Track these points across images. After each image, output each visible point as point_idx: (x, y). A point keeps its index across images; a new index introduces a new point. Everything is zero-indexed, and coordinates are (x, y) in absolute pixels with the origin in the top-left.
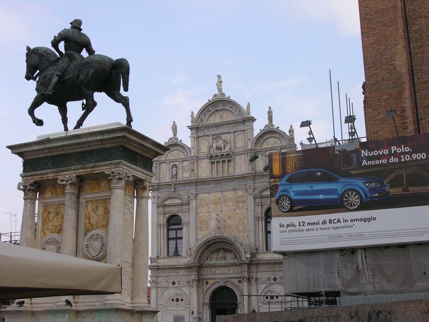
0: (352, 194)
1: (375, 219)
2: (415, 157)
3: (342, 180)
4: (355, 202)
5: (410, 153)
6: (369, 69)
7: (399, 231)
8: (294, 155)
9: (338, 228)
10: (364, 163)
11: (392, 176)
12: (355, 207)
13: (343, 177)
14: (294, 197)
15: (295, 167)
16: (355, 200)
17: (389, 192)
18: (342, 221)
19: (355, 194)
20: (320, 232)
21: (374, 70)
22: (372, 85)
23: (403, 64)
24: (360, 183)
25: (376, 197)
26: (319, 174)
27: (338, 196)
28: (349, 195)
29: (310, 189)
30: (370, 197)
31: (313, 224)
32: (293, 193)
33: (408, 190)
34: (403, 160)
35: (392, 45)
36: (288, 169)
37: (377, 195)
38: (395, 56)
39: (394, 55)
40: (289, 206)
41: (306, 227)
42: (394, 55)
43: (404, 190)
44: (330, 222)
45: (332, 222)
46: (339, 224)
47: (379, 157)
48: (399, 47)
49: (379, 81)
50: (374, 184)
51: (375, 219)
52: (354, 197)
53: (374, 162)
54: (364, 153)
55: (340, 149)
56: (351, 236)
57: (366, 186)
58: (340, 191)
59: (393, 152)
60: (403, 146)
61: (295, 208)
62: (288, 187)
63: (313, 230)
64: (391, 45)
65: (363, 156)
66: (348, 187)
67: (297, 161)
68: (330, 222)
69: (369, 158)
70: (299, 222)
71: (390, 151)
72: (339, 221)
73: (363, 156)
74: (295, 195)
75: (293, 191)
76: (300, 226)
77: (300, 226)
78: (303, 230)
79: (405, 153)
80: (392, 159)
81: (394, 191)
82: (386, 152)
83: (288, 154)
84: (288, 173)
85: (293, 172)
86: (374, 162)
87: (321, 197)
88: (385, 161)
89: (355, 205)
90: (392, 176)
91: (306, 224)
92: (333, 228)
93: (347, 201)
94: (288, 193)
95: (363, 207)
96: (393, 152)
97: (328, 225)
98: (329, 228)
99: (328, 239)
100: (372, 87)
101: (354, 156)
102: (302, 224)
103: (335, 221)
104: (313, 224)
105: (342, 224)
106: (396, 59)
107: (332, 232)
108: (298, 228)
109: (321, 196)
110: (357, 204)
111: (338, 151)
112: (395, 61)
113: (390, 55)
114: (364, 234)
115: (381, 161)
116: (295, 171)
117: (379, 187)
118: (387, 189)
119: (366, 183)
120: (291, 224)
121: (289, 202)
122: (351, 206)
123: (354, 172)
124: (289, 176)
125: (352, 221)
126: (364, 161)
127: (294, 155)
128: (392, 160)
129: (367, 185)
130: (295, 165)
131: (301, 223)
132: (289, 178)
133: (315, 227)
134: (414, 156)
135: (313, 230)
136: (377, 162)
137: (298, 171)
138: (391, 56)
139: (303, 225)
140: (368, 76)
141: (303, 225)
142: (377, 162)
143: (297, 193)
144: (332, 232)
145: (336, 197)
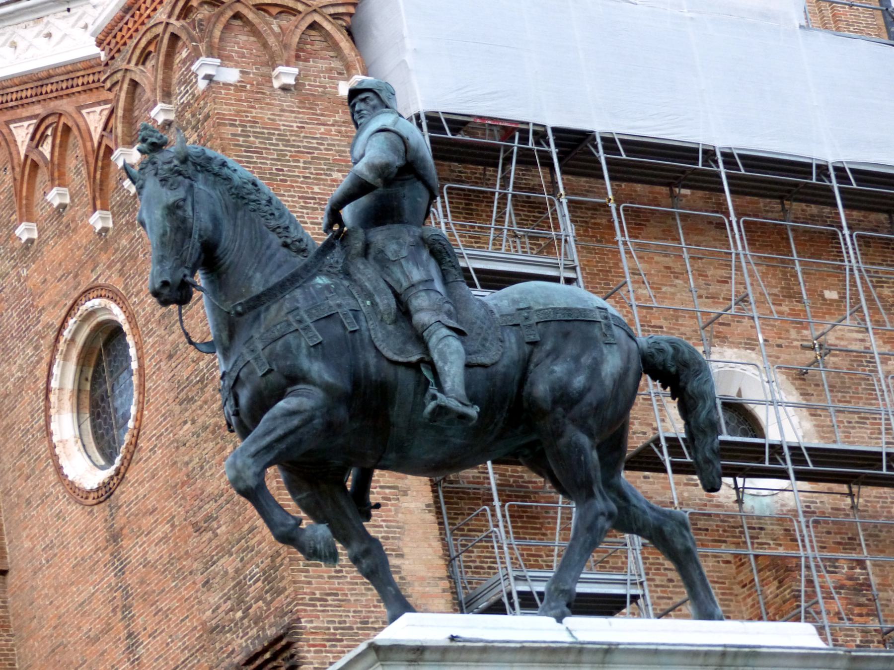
6: (310, 569)
21: (330, 577)
22: (329, 640)
23: (430, 575)
35: (387, 491)
38: (399, 538)
39: (395, 532)
42: (395, 532)
48: (412, 505)
49: (351, 628)
64: (381, 487)
100: (325, 646)
106: (406, 550)
112: (401, 556)
113: (381, 526)
138: (386, 532)
140: (307, 597)
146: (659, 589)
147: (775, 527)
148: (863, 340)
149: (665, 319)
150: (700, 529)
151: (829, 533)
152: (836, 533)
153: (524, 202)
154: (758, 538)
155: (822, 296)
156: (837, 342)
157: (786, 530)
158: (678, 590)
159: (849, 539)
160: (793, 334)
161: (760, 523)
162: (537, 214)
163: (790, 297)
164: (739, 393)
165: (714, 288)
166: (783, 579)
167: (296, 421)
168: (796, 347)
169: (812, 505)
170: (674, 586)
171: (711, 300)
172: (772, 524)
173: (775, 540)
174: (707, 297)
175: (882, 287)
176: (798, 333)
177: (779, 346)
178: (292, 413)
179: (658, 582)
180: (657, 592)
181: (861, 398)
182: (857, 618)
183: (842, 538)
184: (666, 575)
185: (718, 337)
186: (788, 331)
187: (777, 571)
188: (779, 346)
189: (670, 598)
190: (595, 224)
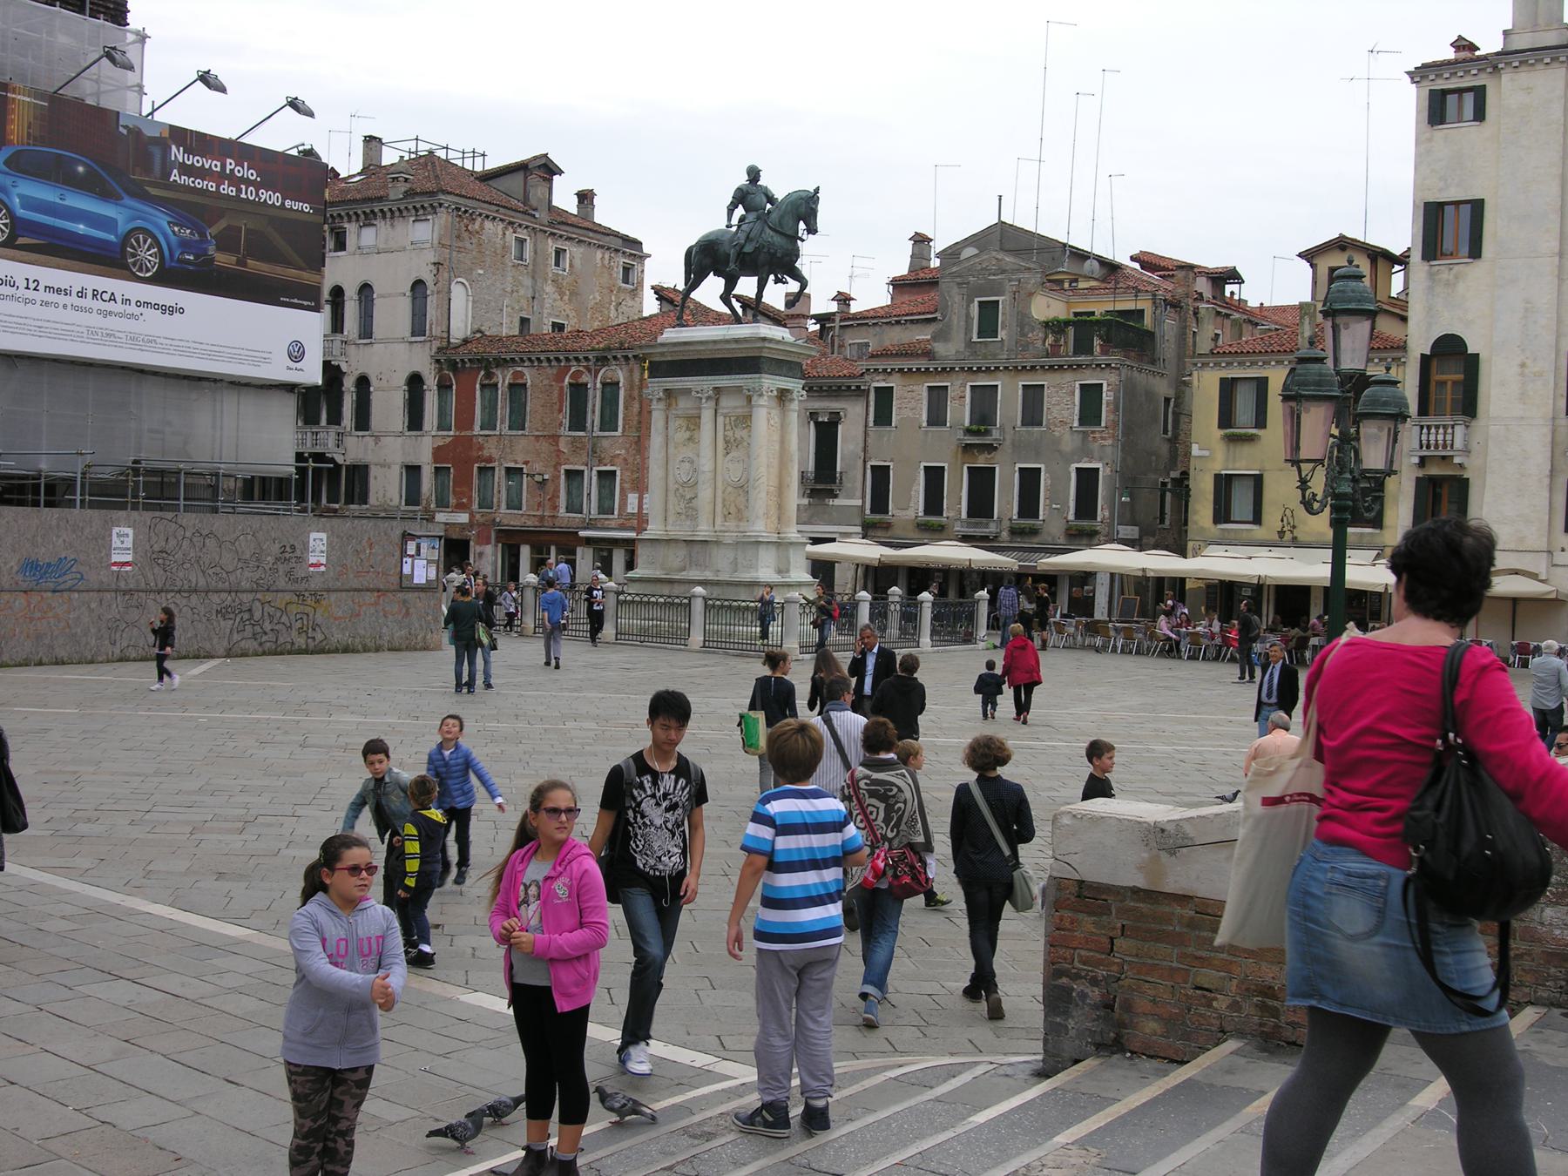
0: (145, 242)
1: (181, 311)
2: (264, 197)
3: (128, 201)
4: (150, 261)
5: (258, 186)
7: (221, 349)
8: (28, 100)
9: (110, 313)
10: (175, 176)
11: (222, 224)
12: (148, 275)
13: (132, 195)
14: (21, 212)
15: (29, 133)
16: (148, 256)
17: (213, 260)
18: (119, 299)
19: (151, 244)
20: (70, 316)
24: (161, 221)
25: (188, 262)
26: (81, 169)
27: (116, 236)
28: (138, 241)
29: (58, 201)
30: (179, 261)
31: (59, 291)
32: (18, 200)
33: (245, 265)
34: (243, 196)
36: (13, 131)
37: (192, 258)
40: (7, 231)
41: (41, 295)
43: (239, 263)
44: (94, 295)
45: (99, 297)
46: (111, 306)
47: (202, 173)
50: (188, 231)
51: (181, 311)
52: (148, 250)
53: (193, 182)
54: (177, 153)
55: (131, 126)
56: (133, 338)
57: (173, 232)
58: (123, 228)
59: (228, 172)
60: (246, 164)
61: (21, 241)
62: (8, 181)
63: (56, 306)
65: (173, 159)
66: (139, 223)
67: (35, 118)
68: (94, 296)
69: (186, 170)
70: (27, 279)
71: (223, 166)
72: (113, 298)
73: (173, 159)
74: (23, 207)
75: (21, 196)
76: (27, 288)
77: (27, 288)
78: (33, 302)
79: (248, 182)
80: (226, 187)
81: (224, 260)
82: (216, 166)
83: (14, 93)
84: (11, 143)
85: (23, 144)
86: (193, 182)
87: (81, 228)
88: (212, 186)
89: (148, 270)
90: (222, 224)
91: (41, 287)
92: (100, 312)
93: (134, 255)
94: (8, 197)
95: (167, 276)
96: (228, 172)
97: (88, 302)
98: (90, 311)
99: (85, 335)
101: (157, 152)
102: (32, 286)
103: (106, 297)
104: (59, 291)
105: (117, 307)
107: (95, 320)
108: (22, 292)
109: (81, 226)
110: (153, 267)
111: (126, 127)
114: (158, 340)
115: (206, 183)
116: (29, 144)
117: (196, 241)
118: (211, 250)
119: (177, 225)
120: (9, 278)
121: (8, 221)
122: (140, 270)
123: (153, 191)
124: (11, 152)
125: (139, 304)
126: (175, 171)
127: (28, 100)
128: (226, 189)
129: (176, 229)
130: (29, 127)
131: (31, 281)
132: (10, 157)
133: (61, 299)
134: (264, 195)
135: (56, 306)
136: (200, 184)
137: (34, 145)
139: (35, 289)
141: (35, 289)
142: (200, 184)
143: (29, 204)
144: (95, 320)
145: (112, 238)
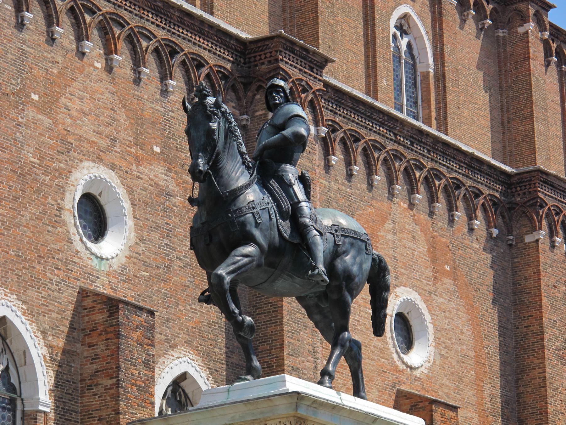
146: (43, 299)
147: (105, 278)
148: (166, 181)
149: (75, 140)
150: (69, 270)
151: (129, 289)
152: (132, 290)
153: (19, 48)
154: (95, 282)
155: (152, 148)
156: (154, 178)
157: (109, 281)
158: (52, 302)
159: (138, 295)
160: (134, 167)
161: (98, 274)
162: (24, 58)
163: (137, 145)
164: (100, 195)
165: (102, 128)
166: (114, 313)
167: (246, 260)
168: (133, 175)
169: (124, 271)
170: (51, 300)
171: (99, 135)
172: (103, 276)
173: (103, 286)
174: (97, 133)
175: (181, 152)
176: (137, 167)
177: (127, 172)
178: (246, 256)
179: (43, 295)
180: (41, 300)
181: (159, 215)
182: (145, 346)
183: (135, 294)
184: (48, 292)
185: (99, 158)
186: (132, 165)
187: (110, 307)
188: (127, 172)
189: (47, 306)
190: (51, 72)
